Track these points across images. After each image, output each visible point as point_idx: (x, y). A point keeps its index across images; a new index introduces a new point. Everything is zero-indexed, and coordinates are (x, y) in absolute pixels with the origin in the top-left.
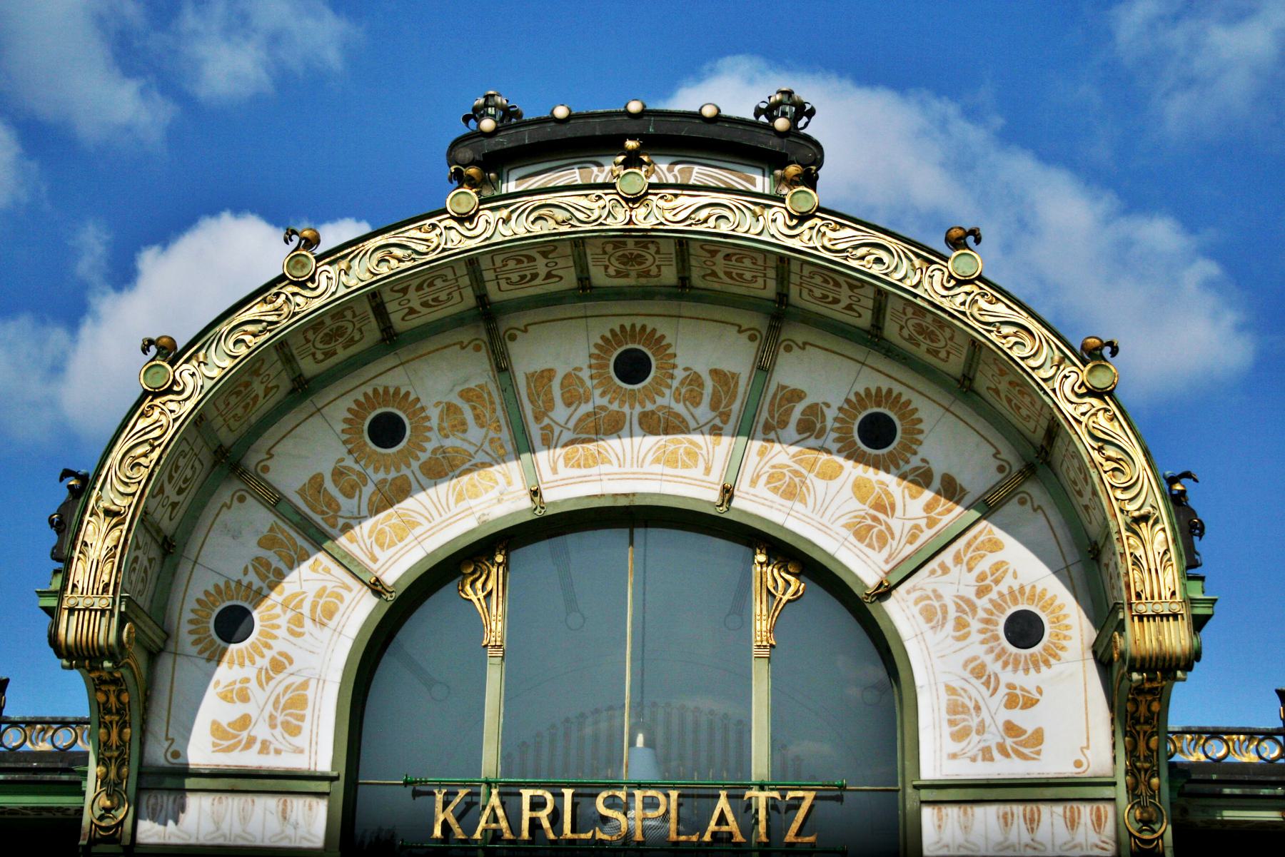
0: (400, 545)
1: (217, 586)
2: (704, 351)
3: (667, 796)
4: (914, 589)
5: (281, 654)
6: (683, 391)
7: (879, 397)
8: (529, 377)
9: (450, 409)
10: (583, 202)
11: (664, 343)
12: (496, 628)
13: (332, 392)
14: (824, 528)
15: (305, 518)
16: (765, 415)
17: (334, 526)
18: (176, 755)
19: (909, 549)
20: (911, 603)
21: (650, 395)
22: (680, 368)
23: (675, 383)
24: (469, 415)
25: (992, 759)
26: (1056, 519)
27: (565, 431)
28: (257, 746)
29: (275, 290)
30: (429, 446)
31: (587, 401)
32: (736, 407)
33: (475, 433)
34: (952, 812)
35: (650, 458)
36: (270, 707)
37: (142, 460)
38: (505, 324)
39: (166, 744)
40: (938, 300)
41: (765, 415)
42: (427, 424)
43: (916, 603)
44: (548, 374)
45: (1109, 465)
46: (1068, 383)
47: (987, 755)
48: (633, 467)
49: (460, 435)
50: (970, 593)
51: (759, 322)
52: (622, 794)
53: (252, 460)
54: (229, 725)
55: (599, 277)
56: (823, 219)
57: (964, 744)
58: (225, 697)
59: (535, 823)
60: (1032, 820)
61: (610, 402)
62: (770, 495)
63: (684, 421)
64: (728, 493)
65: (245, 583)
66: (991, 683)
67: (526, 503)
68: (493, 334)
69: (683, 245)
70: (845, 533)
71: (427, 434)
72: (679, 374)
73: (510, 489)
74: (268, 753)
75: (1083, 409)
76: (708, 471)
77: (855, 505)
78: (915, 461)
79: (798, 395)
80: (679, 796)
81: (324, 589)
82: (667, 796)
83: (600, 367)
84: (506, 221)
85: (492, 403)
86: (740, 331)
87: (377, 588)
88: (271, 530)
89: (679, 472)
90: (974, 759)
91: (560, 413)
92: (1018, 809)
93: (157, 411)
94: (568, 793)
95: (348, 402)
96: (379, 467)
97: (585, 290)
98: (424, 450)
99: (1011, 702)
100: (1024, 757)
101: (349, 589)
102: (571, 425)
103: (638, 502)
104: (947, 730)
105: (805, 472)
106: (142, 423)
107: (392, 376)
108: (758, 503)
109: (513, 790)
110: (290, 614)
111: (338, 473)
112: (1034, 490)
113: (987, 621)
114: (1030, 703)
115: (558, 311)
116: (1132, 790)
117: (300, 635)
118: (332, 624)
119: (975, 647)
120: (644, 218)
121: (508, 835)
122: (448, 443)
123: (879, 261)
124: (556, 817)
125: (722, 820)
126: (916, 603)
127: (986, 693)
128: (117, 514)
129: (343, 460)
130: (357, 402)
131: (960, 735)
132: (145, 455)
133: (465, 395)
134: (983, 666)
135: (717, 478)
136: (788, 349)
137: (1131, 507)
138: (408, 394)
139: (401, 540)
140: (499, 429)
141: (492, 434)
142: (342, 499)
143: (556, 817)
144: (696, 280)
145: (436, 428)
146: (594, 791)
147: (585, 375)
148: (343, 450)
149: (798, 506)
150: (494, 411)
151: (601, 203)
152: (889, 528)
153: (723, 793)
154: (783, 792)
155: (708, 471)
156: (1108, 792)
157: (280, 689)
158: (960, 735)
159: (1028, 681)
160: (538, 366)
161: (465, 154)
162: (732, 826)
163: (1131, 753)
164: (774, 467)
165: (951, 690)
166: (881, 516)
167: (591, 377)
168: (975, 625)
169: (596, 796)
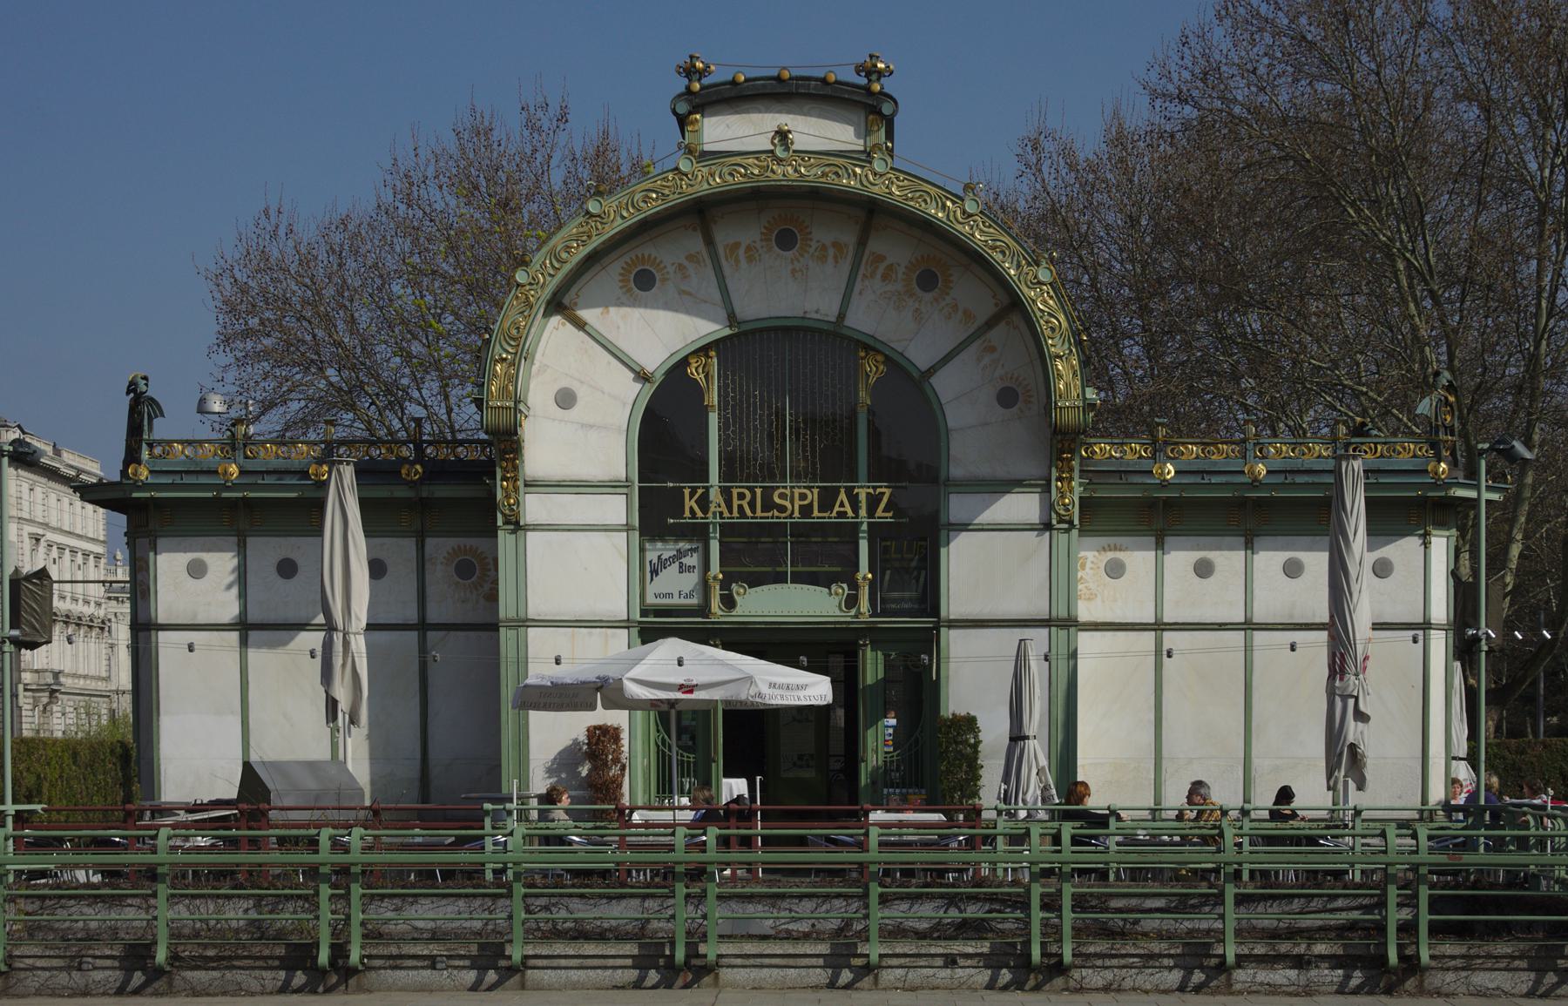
9: (681, 267)
12: (713, 397)
52: (788, 492)
59: (740, 507)
72: (814, 244)
79: (880, 258)
87: (642, 376)
94: (759, 491)
108: (862, 320)
121: (726, 514)
124: (752, 505)
125: (842, 505)
133: (690, 258)
143: (752, 505)
154: (875, 488)
162: (848, 509)
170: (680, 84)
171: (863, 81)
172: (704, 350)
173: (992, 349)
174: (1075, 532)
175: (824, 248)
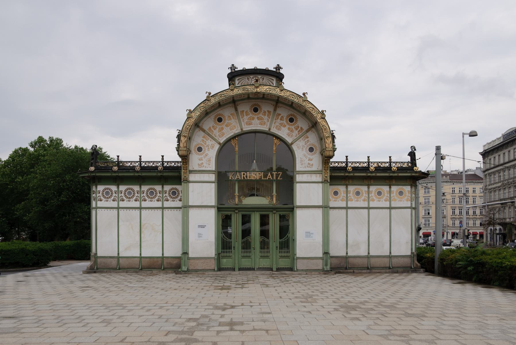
2: (266, 107)
7: (292, 115)
9: (229, 116)
13: (211, 114)
14: (283, 134)
21: (258, 114)
26: (316, 134)
33: (233, 120)
34: (301, 175)
38: (237, 103)
44: (243, 111)
47: (305, 167)
48: (256, 125)
50: (304, 144)
51: (275, 103)
55: (251, 96)
58: (200, 160)
59: (244, 177)
64: (270, 129)
68: (235, 104)
77: (288, 131)
79: (280, 115)
87: (219, 143)
91: (245, 117)
96: (219, 126)
97: (249, 98)
99: (309, 160)
107: (220, 111)
108: (274, 131)
111: (213, 127)
112: (313, 129)
114: (311, 160)
119: (304, 152)
124: (246, 176)
135: (268, 127)
144: (265, 97)
148: (213, 123)
158: (302, 165)
159: (311, 157)
161: (230, 76)
162: (271, 177)
163: (325, 167)
168: (304, 149)
170: (230, 71)
171: (275, 70)
172: (234, 137)
173: (308, 137)
174: (329, 184)
175: (265, 112)
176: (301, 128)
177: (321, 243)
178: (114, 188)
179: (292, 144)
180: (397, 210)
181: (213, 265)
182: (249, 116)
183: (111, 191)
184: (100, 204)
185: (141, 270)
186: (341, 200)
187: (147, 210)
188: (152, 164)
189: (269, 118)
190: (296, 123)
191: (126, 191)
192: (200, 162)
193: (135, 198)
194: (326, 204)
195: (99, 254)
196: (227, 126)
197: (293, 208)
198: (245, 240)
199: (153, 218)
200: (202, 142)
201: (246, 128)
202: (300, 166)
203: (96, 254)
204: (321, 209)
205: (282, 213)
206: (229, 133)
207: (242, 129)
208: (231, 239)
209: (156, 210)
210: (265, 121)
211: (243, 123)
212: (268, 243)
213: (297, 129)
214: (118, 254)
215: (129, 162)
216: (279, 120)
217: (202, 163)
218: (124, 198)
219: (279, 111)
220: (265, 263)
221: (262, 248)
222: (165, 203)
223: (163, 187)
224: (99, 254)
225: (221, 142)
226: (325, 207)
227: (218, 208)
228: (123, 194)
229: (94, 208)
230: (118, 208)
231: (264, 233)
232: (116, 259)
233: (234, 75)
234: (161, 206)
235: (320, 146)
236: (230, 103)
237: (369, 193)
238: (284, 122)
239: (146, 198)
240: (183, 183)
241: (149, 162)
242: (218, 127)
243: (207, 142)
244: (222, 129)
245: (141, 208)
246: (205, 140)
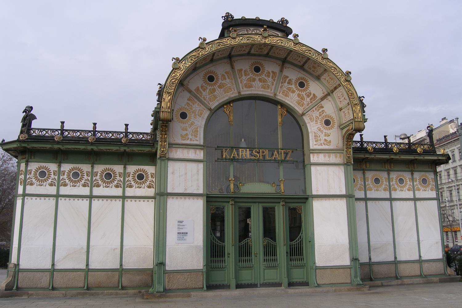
0: (214, 101)
1: (180, 108)
2: (270, 67)
3: (266, 151)
4: (308, 114)
5: (193, 122)
6: (267, 75)
8: (238, 70)
9: (223, 75)
10: (256, 37)
11: (263, 65)
15: (196, 95)
16: (281, 80)
17: (201, 97)
18: (174, 141)
19: (307, 107)
20: (307, 117)
22: (266, 70)
23: (265, 73)
24: (227, 77)
25: (322, 145)
27: (245, 81)
28: (189, 139)
29: (198, 50)
30: (219, 82)
31: (249, 76)
32: (276, 78)
33: (228, 80)
34: (316, 155)
35: (260, 87)
36: (191, 132)
37: (174, 82)
38: (233, 59)
39: (172, 138)
40: (321, 62)
41: (281, 80)
42: (219, 78)
43: (309, 117)
44: (241, 70)
45: (350, 94)
46: (343, 79)
47: (321, 145)
48: (257, 89)
49: (225, 80)
51: (280, 63)
52: (258, 150)
53: (185, 83)
54: (184, 135)
56: (300, 45)
57: (317, 143)
58: (183, 130)
60: (329, 156)
61: (253, 76)
62: (282, 95)
63: (267, 80)
65: (185, 107)
66: (322, 132)
67: (237, 95)
68: (231, 60)
69: (272, 46)
70: (296, 103)
71: (219, 80)
72: (266, 72)
73: (235, 92)
74: (192, 141)
75: (346, 84)
76: (271, 90)
77: (298, 98)
78: (308, 91)
79: (287, 77)
80: (268, 151)
81: (200, 109)
82: (266, 151)
83: (251, 69)
84: (242, 39)
85: (231, 74)
86: (277, 64)
87: (210, 109)
88: (190, 97)
89: (266, 90)
90: (319, 145)
91: (244, 77)
92: (327, 154)
93: (176, 73)
95: (203, 73)
97: (249, 54)
98: (218, 83)
99: (325, 135)
100: (328, 145)
101: (205, 110)
102: (246, 80)
103: (259, 96)
104: (314, 140)
105: (289, 92)
106: (174, 75)
107: (212, 68)
108: (280, 97)
109: (238, 149)
110: (194, 114)
111: (202, 87)
113: (321, 121)
115: (243, 57)
116: (347, 151)
117: (196, 118)
118: (202, 116)
120: (267, 41)
122: (223, 82)
123: (310, 53)
126: (309, 117)
127: (321, 134)
128: (170, 93)
129: (203, 84)
130: (205, 73)
131: (316, 141)
132: (175, 81)
133: (226, 73)
134: (320, 129)
135: (272, 91)
136: (286, 68)
137: (353, 102)
138: (215, 72)
139: (214, 100)
140: (232, 80)
141: (231, 81)
142: (203, 92)
145: (220, 79)
146: (252, 149)
147: (248, 70)
149: (287, 98)
150: (231, 76)
151: (259, 37)
152: (304, 103)
153: (276, 150)
155: (271, 90)
156: (342, 152)
157: (193, 128)
160: (240, 68)
162: (278, 156)
163: (347, 145)
164: (283, 90)
165: (315, 133)
166: (302, 101)
167: (250, 71)
168: (319, 121)
169: (253, 150)
173: (322, 107)
174: (352, 167)
176: (314, 95)
177: (348, 245)
178: (53, 167)
179: (303, 114)
180: (425, 201)
181: (201, 281)
182: (249, 77)
183: (49, 171)
184: (30, 189)
185: (88, 289)
186: (358, 189)
187: (101, 200)
188: (111, 135)
189: (274, 80)
190: (307, 89)
191: (70, 172)
192: (184, 133)
193: (83, 181)
194: (350, 193)
195: (21, 267)
196: (220, 87)
197: (307, 199)
198: (243, 243)
199: (107, 212)
200: (186, 106)
201: (246, 92)
202: (315, 143)
203: (18, 264)
204: (345, 198)
205: (293, 205)
206: (222, 96)
207: (239, 93)
208: (224, 242)
209: (114, 200)
210: (269, 84)
211: (240, 85)
212: (275, 248)
213: (308, 96)
214: (53, 265)
215: (78, 131)
216: (286, 84)
217: (187, 134)
218: (67, 181)
219: (286, 72)
220: (271, 275)
221: (266, 254)
222: (128, 189)
223: (125, 168)
224: (21, 267)
225: (213, 107)
226: (349, 196)
227: (207, 197)
228: (65, 176)
229: (20, 196)
230: (57, 196)
231: (269, 231)
232: (48, 274)
233: (230, 24)
234: (121, 195)
235: (338, 118)
236: (224, 58)
237: (389, 180)
238: (293, 86)
239: (100, 182)
240: (159, 161)
241: (107, 132)
242: (209, 88)
243: (194, 106)
244: (214, 90)
245: (91, 197)
246: (191, 104)
